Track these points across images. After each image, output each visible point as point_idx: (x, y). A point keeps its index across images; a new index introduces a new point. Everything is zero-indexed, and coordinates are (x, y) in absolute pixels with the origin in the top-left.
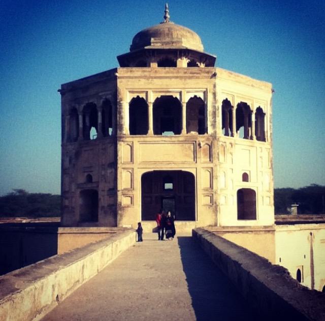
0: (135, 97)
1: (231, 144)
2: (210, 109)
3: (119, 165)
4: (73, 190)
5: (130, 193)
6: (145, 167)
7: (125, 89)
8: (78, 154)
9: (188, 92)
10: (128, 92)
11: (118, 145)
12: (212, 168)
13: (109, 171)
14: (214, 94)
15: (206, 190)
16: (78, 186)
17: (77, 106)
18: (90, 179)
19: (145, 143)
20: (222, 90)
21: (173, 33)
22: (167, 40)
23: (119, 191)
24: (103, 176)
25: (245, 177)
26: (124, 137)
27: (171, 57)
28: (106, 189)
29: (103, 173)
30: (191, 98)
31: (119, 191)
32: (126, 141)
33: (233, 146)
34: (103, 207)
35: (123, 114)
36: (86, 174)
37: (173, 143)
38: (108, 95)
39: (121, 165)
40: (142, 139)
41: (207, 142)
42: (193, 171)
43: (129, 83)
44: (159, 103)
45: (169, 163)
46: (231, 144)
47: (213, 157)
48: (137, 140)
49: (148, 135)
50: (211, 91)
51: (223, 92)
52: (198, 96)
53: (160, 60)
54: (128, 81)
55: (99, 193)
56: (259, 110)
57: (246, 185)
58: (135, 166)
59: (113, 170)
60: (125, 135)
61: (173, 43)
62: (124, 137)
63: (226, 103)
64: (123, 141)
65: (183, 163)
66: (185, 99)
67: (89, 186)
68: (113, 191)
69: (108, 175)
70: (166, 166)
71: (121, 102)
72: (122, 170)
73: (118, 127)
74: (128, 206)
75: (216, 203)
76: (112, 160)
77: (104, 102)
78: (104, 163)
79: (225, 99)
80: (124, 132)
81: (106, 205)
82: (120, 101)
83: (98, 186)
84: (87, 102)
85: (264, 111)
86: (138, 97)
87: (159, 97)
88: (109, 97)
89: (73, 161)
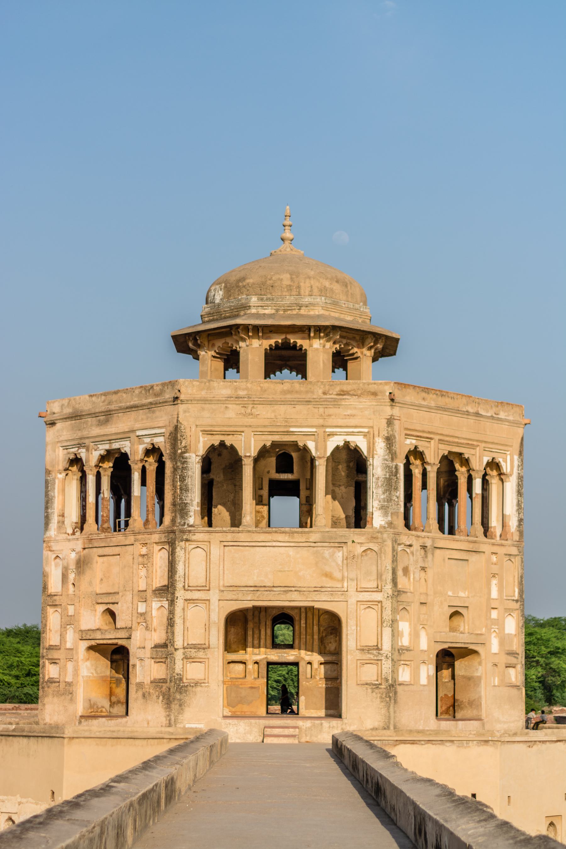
0: (217, 443)
1: (424, 547)
2: (377, 469)
3: (180, 594)
4: (69, 645)
5: (201, 654)
6: (234, 597)
7: (193, 429)
8: (82, 564)
9: (331, 435)
10: (201, 433)
11: (178, 549)
12: (381, 601)
13: (155, 605)
15: (364, 650)
16: (83, 635)
17: (83, 453)
19: (236, 544)
20: (407, 429)
21: (302, 284)
22: (289, 300)
23: (176, 650)
24: (142, 614)
26: (190, 532)
28: (149, 645)
29: (142, 608)
30: (337, 448)
31: (176, 650)
32: (194, 541)
33: (430, 556)
34: (140, 685)
35: (188, 481)
38: (156, 435)
39: (182, 592)
40: (229, 537)
41: (371, 546)
43: (206, 414)
45: (287, 589)
46: (424, 547)
47: (384, 577)
49: (241, 528)
50: (381, 435)
51: (406, 435)
52: (352, 445)
53: (270, 345)
54: (203, 409)
55: (132, 651)
59: (166, 604)
60: (191, 526)
61: (300, 307)
62: (190, 532)
64: (187, 540)
65: (317, 590)
67: (111, 637)
68: (164, 650)
69: (154, 613)
70: (283, 597)
71: (187, 455)
72: (186, 603)
74: (197, 684)
75: (387, 680)
76: (165, 582)
78: (142, 587)
79: (412, 449)
80: (191, 521)
81: (147, 681)
82: (183, 453)
83: (129, 638)
84: (107, 447)
85: (506, 467)
86: (222, 444)
87: (268, 444)
88: (160, 441)
89: (72, 576)
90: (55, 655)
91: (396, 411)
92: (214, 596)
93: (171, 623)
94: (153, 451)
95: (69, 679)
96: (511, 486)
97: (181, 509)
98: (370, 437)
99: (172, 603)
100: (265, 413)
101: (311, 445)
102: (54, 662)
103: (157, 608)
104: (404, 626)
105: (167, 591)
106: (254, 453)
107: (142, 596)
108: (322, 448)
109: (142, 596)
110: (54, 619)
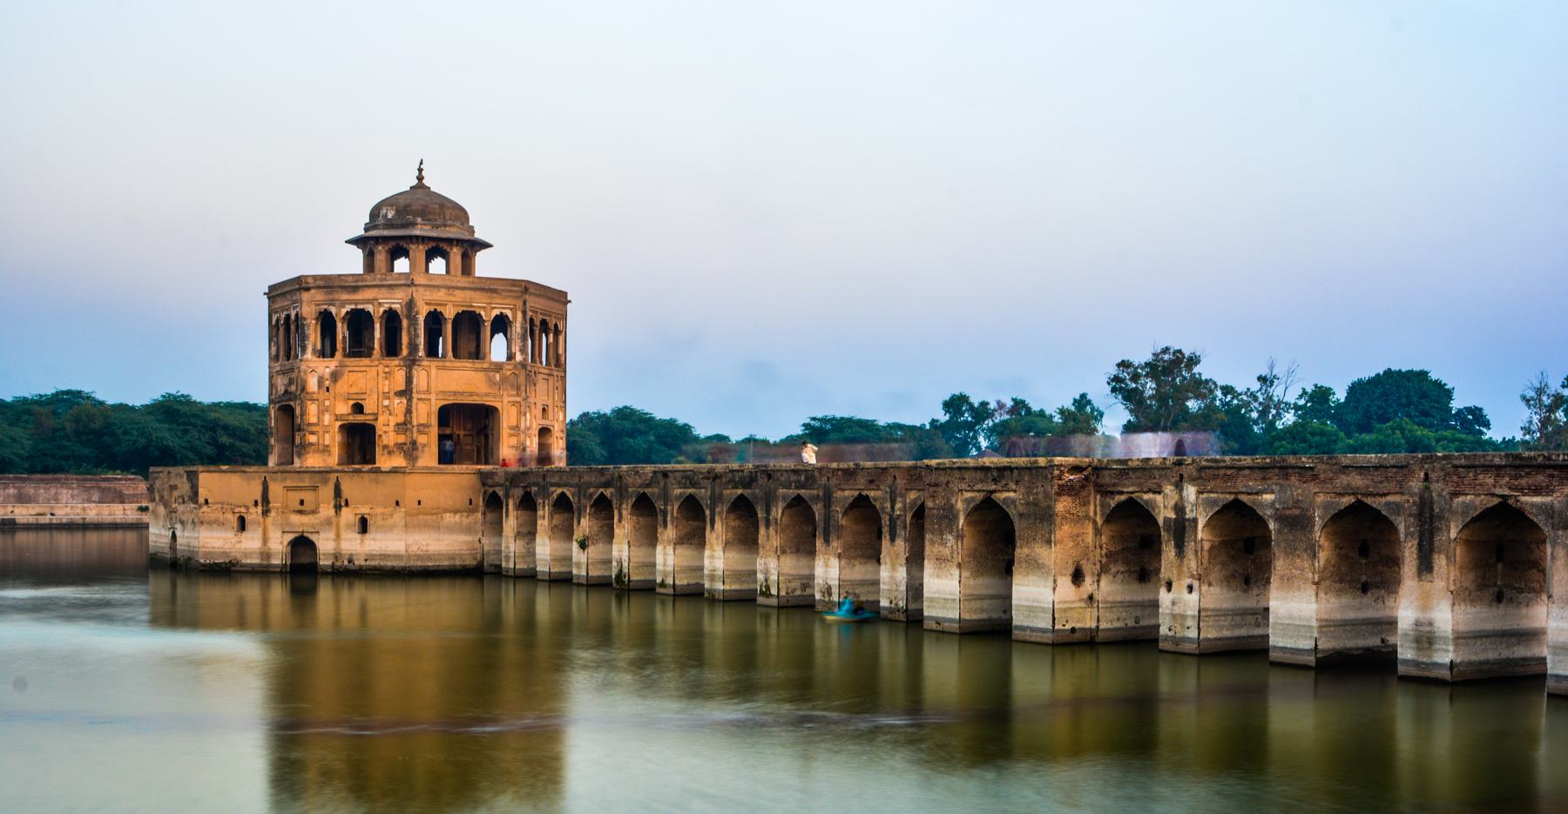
3: (415, 396)
8: (335, 376)
13: (397, 401)
15: (511, 428)
17: (333, 310)
18: (358, 408)
19: (444, 368)
27: (445, 246)
28: (392, 424)
29: (386, 403)
34: (385, 447)
37: (476, 370)
44: (459, 318)
45: (472, 394)
48: (432, 364)
57: (545, 423)
58: (433, 397)
65: (487, 395)
67: (360, 418)
73: (413, 347)
85: (560, 327)
88: (397, 307)
90: (314, 429)
92: (433, 397)
93: (409, 411)
96: (561, 338)
99: (410, 400)
100: (459, 296)
103: (399, 404)
105: (406, 393)
107: (386, 396)
109: (386, 396)
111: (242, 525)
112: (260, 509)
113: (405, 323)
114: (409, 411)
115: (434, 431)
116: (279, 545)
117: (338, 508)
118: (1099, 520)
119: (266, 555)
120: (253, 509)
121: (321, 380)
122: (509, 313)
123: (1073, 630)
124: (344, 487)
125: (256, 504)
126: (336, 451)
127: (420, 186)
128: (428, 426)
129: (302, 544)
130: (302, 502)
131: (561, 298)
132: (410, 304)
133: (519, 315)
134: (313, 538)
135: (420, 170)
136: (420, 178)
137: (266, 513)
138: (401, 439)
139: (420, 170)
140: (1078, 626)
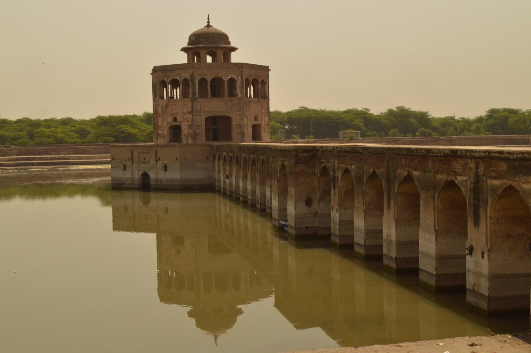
2: (238, 84)
3: (195, 113)
13: (188, 116)
14: (242, 77)
15: (238, 125)
17: (166, 80)
18: (175, 119)
24: (185, 118)
25: (256, 118)
28: (187, 125)
29: (185, 117)
34: (185, 135)
36: (173, 117)
42: (231, 116)
44: (213, 81)
56: (263, 81)
59: (191, 116)
63: (247, 80)
66: (226, 79)
67: (176, 124)
77: (184, 79)
85: (265, 81)
88: (187, 77)
89: (164, 110)
91: (243, 70)
94: (185, 80)
95: (165, 133)
97: (194, 93)
98: (237, 76)
101: (224, 78)
102: (160, 130)
103: (189, 116)
104: (245, 120)
105: (191, 113)
106: (210, 80)
108: (226, 79)
110: (160, 120)
111: (125, 168)
112: (131, 161)
113: (190, 84)
114: (193, 120)
115: (204, 128)
116: (137, 175)
117: (156, 161)
118: (319, 175)
119: (133, 180)
120: (128, 162)
121: (162, 108)
122: (235, 77)
123: (307, 228)
124: (158, 153)
125: (129, 160)
126: (168, 137)
127: (208, 26)
128: (201, 126)
129: (145, 176)
130: (145, 159)
131: (266, 69)
132: (192, 76)
133: (240, 78)
134: (149, 173)
135: (208, 19)
136: (208, 22)
137: (133, 163)
138: (191, 131)
139: (208, 19)
140: (310, 225)
